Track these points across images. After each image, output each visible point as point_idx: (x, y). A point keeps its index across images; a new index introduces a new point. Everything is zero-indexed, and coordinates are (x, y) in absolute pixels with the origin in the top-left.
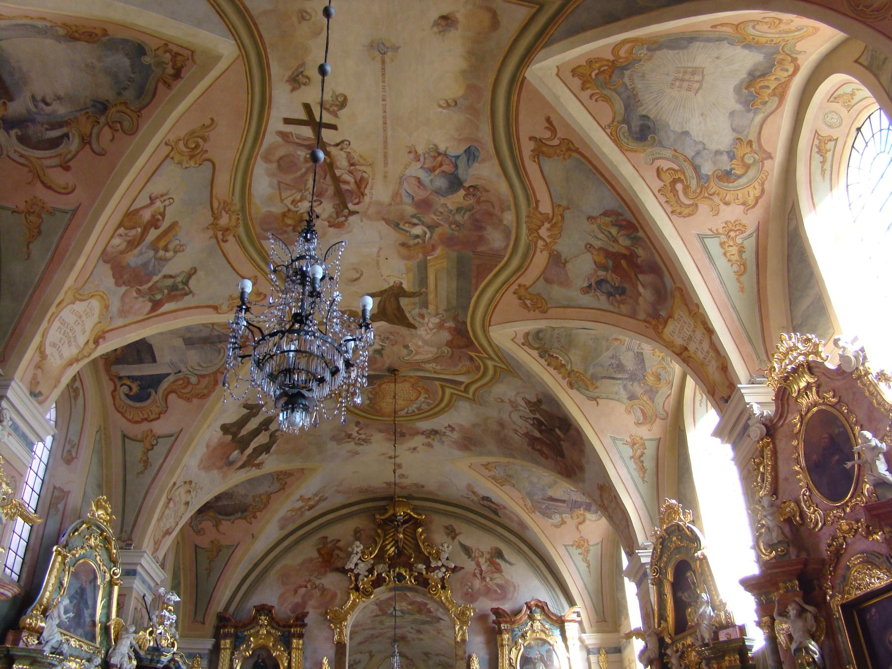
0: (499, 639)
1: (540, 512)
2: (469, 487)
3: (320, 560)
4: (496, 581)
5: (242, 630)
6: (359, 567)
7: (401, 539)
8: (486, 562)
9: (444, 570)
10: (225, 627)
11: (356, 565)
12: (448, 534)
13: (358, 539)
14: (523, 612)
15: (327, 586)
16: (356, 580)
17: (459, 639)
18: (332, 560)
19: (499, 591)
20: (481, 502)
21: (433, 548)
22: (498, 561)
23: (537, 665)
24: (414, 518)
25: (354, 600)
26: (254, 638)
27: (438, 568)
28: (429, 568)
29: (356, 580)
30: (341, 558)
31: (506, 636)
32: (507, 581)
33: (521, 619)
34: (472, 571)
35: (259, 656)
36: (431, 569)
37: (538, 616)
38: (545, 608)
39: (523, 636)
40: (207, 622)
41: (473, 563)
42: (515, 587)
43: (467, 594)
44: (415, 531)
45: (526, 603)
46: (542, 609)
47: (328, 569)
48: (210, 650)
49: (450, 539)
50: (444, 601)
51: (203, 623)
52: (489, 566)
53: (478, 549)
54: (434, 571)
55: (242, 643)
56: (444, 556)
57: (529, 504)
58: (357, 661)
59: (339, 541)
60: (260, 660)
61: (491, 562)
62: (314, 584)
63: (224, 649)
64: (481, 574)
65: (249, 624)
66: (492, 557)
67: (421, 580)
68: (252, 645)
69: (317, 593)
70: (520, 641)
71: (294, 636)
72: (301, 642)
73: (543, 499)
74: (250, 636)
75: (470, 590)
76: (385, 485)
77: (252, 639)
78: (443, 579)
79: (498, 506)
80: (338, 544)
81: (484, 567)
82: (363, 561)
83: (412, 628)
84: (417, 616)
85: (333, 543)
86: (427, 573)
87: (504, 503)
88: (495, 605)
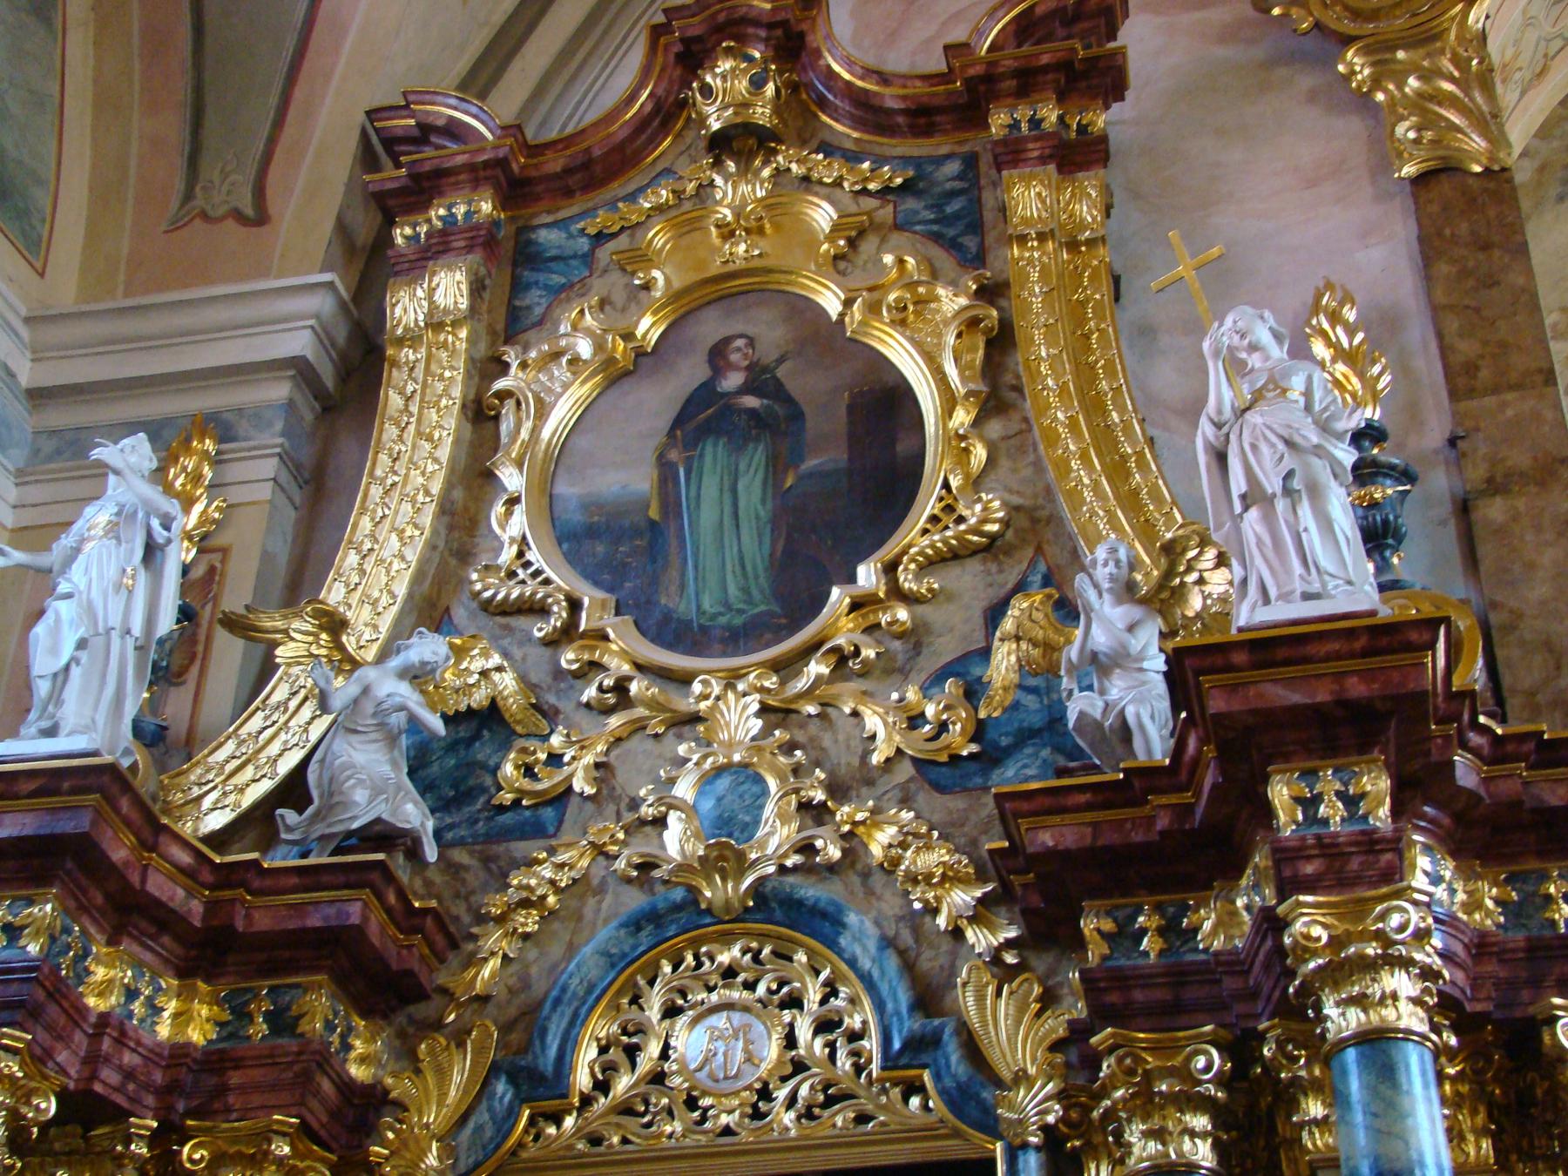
35: (718, 355)
40: (287, 206)
48: (299, 368)
51: (261, 218)
60: (733, 381)
71: (1010, 153)
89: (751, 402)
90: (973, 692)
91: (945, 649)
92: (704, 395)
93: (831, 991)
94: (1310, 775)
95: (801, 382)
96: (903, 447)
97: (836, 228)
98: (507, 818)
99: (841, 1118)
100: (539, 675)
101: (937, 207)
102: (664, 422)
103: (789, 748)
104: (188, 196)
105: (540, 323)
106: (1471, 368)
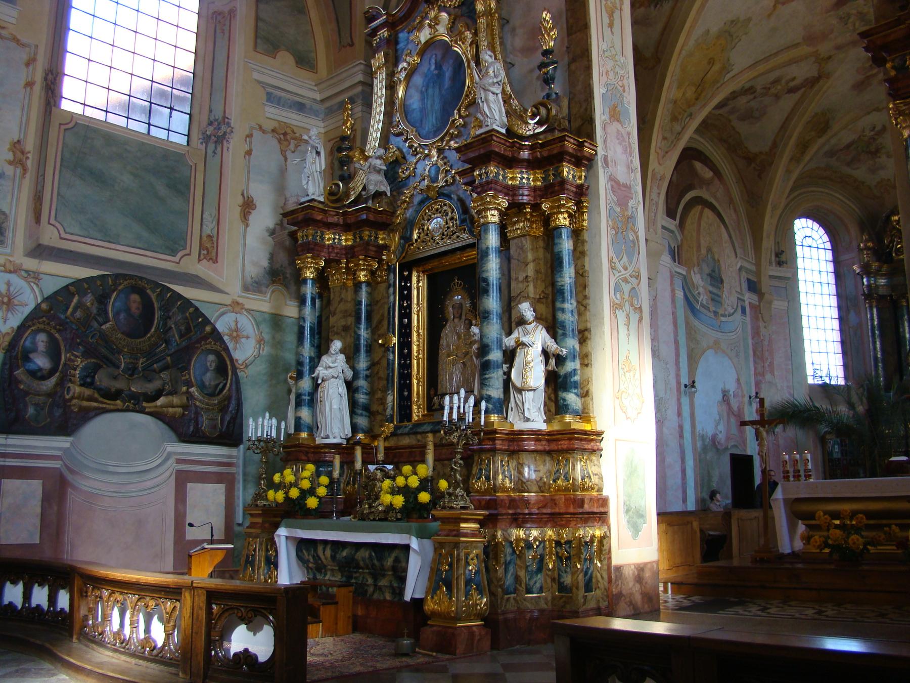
58: (878, 128)
98: (401, 184)
104: (340, 42)
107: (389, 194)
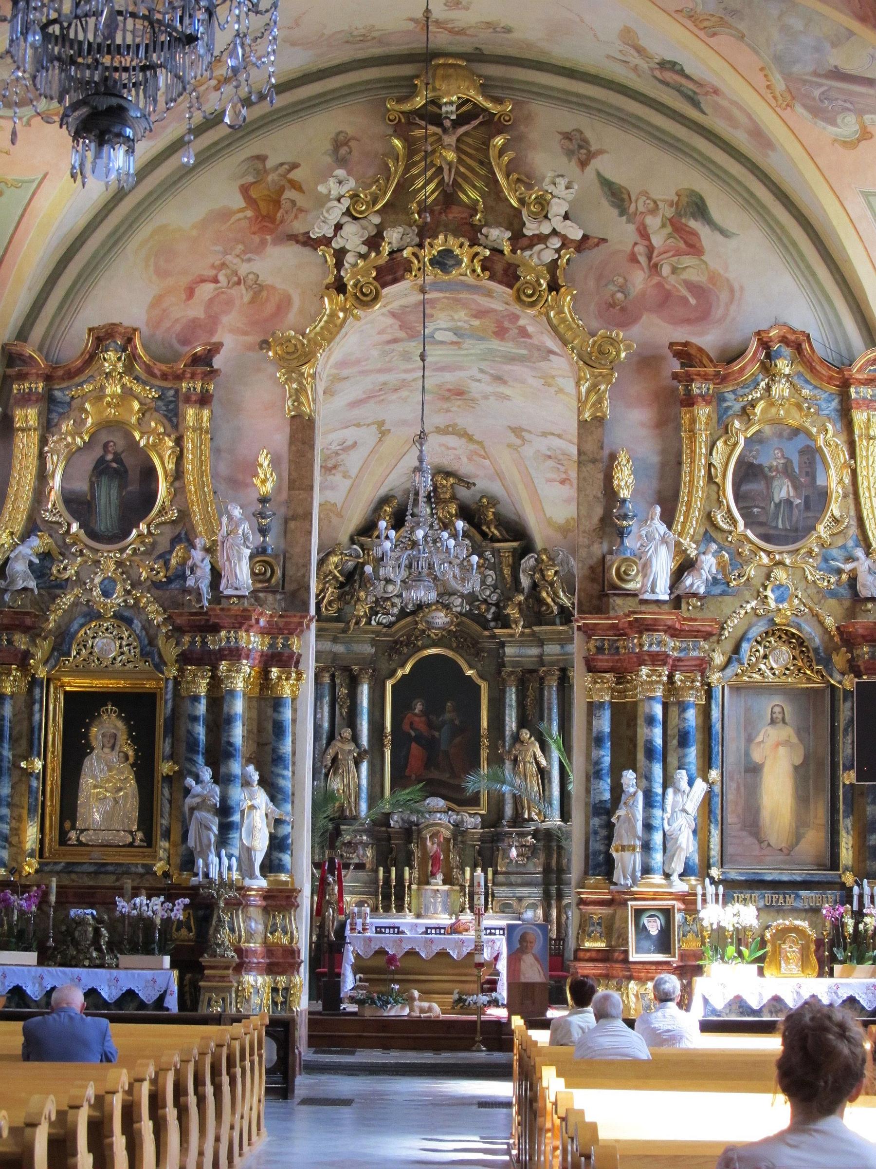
0: (685, 421)
1: (805, 106)
2: (628, 36)
3: (249, 213)
4: (685, 276)
5: (64, 385)
6: (343, 232)
7: (450, 164)
8: (663, 226)
9: (558, 245)
10: (22, 377)
11: (338, 227)
12: (570, 153)
13: (342, 162)
14: (750, 354)
15: (266, 278)
16: (339, 265)
17: (587, 415)
18: (279, 215)
19: (693, 301)
20: (657, 73)
21: (529, 187)
22: (693, 224)
23: (776, 483)
24: (485, 110)
25: (333, 315)
26: (92, 405)
27: (541, 239)
28: (518, 238)
29: (339, 265)
30: (301, 210)
31: (703, 412)
32: (713, 278)
33: (742, 369)
34: (629, 249)
35: (106, 446)
36: (524, 242)
37: (784, 366)
38: (806, 346)
39: (745, 413)
41: (631, 228)
42: (732, 291)
43: (612, 305)
44: (487, 143)
45: (758, 333)
46: (798, 348)
47: (268, 237)
49: (574, 165)
50: (555, 321)
52: (670, 236)
53: (645, 194)
54: (531, 246)
55: (63, 416)
56: (558, 208)
57: (780, 85)
58: (349, 443)
59: (294, 166)
60: (110, 457)
61: (677, 228)
62: (236, 273)
63: (23, 430)
64: (650, 258)
65: (80, 371)
66: (679, 214)
67: (499, 267)
68: (90, 421)
69: (243, 295)
70: (737, 424)
72: (206, 413)
73: (815, 74)
74: (84, 397)
75: (620, 296)
76: (411, 26)
77: (87, 406)
78: (553, 266)
79: (700, 85)
80: (291, 176)
81: (657, 240)
82: (355, 218)
83: (481, 371)
84: (495, 344)
85: (282, 170)
86: (514, 251)
87: (716, 82)
88: (680, 334)
89: (114, 465)
90: (167, 563)
91: (160, 549)
92: (101, 461)
93: (130, 636)
94: (229, 632)
95: (129, 461)
96: (153, 486)
97: (139, 410)
99: (130, 665)
100: (60, 543)
101: (167, 405)
102: (91, 467)
103: (122, 573)
105: (56, 425)
106: (294, 481)
107: (36, 592)
